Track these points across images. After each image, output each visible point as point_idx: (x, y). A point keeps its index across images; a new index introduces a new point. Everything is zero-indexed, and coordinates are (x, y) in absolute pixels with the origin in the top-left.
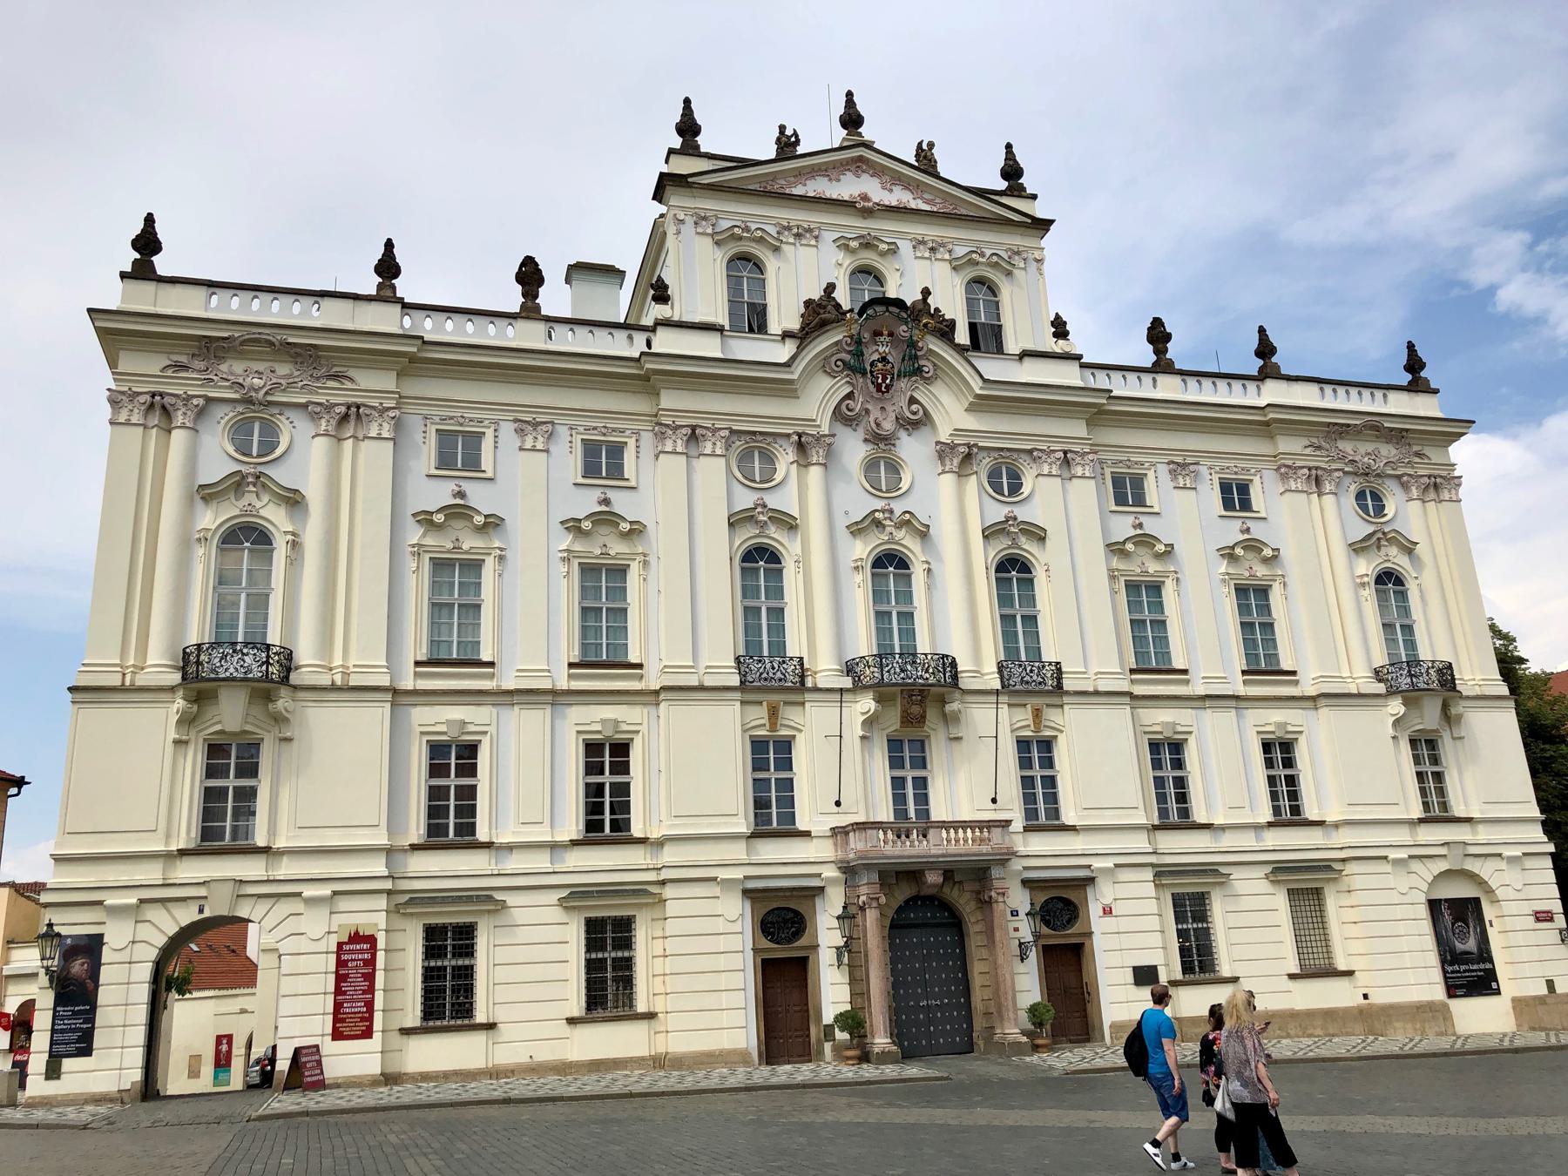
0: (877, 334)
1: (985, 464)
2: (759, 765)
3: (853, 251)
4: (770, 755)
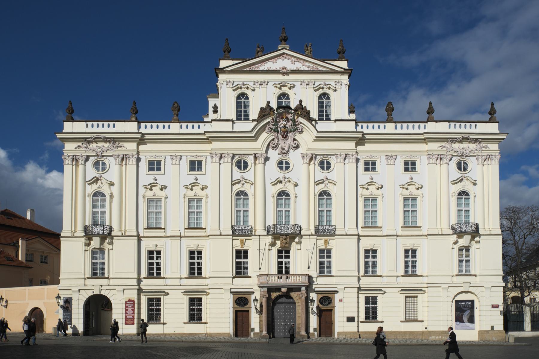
2: (238, 257)
4: (241, 254)
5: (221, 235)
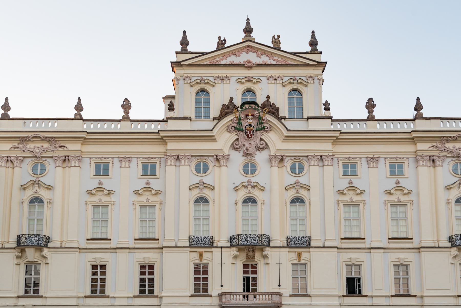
0: (247, 115)
1: (288, 163)
2: (197, 272)
3: (243, 83)
5: (176, 247)
